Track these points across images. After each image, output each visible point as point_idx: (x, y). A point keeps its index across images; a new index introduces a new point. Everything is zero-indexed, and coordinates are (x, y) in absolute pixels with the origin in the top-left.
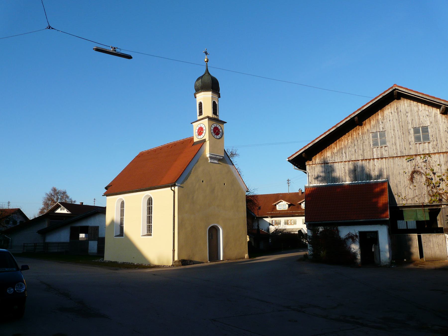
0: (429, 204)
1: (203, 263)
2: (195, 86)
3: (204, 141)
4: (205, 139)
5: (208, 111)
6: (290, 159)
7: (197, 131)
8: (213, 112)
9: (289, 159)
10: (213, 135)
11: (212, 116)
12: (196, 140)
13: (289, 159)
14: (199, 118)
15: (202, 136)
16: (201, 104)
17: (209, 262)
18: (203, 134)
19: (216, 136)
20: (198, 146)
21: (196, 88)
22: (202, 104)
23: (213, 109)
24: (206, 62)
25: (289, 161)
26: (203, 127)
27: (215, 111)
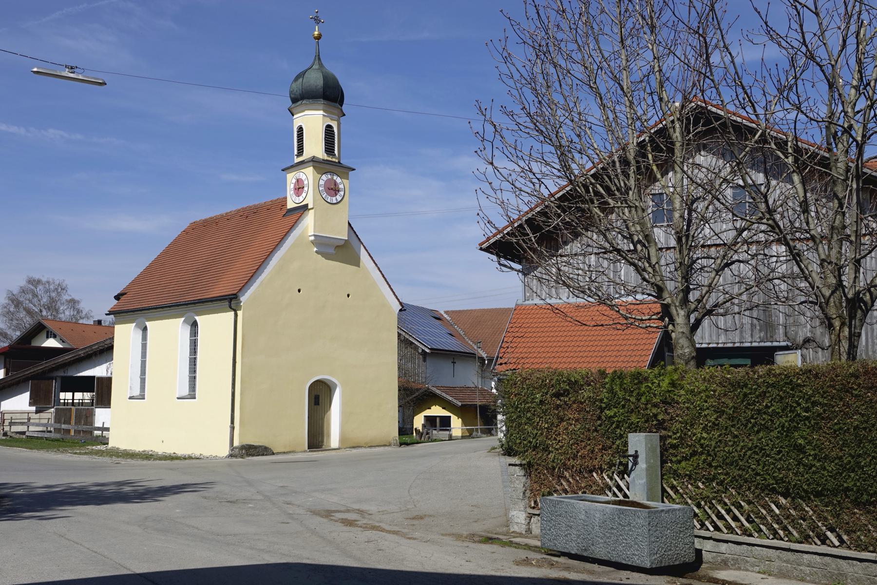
0: (711, 561)
1: (293, 452)
2: (291, 92)
3: (305, 208)
4: (307, 205)
5: (315, 147)
6: (484, 246)
7: (292, 186)
8: (326, 148)
9: (482, 246)
10: (324, 196)
11: (323, 155)
12: (290, 205)
13: (482, 246)
14: (297, 160)
15: (301, 198)
16: (300, 129)
17: (308, 450)
18: (304, 195)
19: (329, 197)
20: (294, 217)
21: (293, 96)
22: (303, 130)
23: (325, 142)
24: (316, 38)
25: (481, 249)
26: (303, 179)
27: (329, 148)
